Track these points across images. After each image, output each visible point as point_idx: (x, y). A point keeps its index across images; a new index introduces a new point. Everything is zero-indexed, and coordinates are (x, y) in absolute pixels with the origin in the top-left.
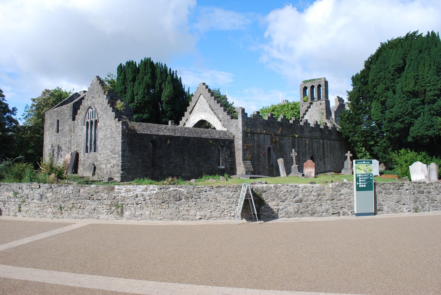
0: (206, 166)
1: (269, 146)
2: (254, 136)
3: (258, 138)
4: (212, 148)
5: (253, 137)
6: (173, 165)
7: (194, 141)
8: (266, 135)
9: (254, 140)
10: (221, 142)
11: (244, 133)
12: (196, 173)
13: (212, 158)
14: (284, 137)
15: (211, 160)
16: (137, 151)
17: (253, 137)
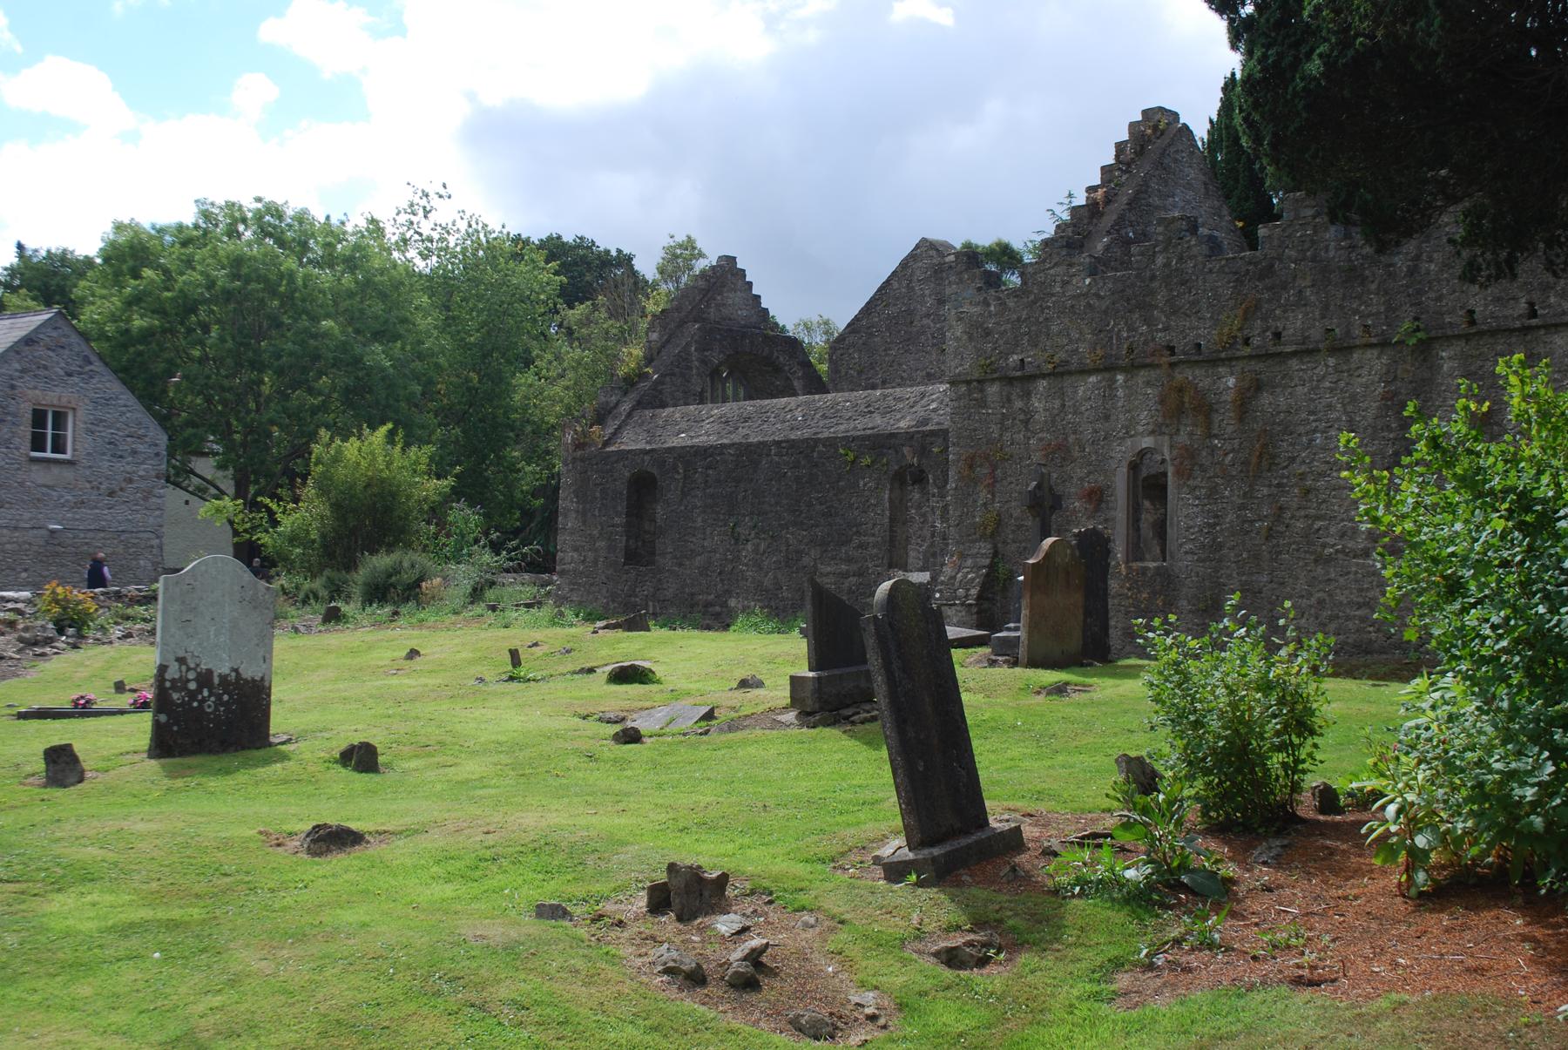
0: (829, 569)
1: (1147, 442)
2: (1027, 395)
3: (1057, 403)
4: (861, 483)
5: (1019, 404)
6: (698, 560)
7: (776, 459)
8: (1120, 378)
9: (1026, 422)
10: (906, 450)
11: (963, 388)
12: (783, 599)
13: (858, 533)
14: (1294, 363)
15: (856, 541)
16: (597, 513)
17: (1019, 404)
